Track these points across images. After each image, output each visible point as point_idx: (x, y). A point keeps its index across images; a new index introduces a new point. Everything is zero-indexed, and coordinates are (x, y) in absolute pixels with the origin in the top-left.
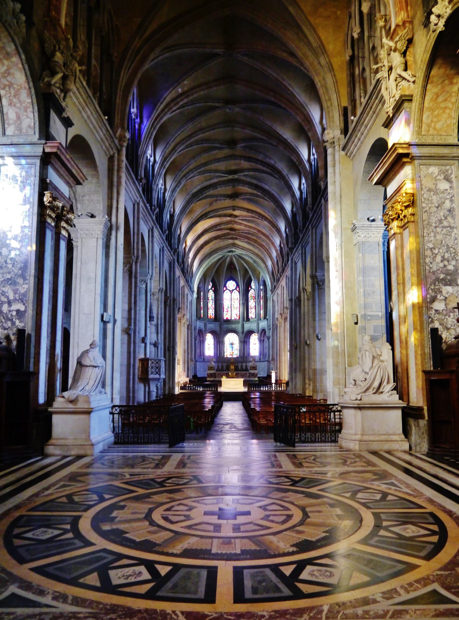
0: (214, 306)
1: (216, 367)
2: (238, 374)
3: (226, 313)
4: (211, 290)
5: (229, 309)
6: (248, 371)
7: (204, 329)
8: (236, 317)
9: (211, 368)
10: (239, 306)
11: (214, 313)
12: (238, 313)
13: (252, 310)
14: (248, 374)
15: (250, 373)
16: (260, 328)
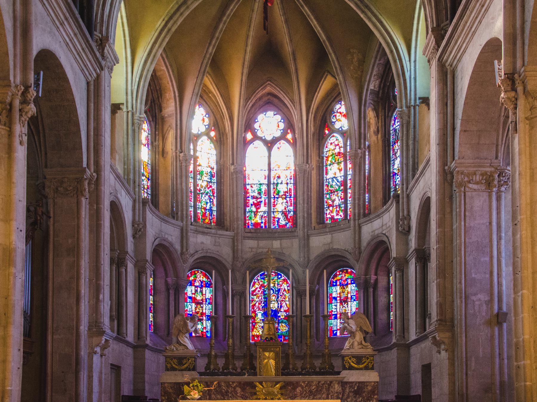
0: (214, 187)
1: (202, 363)
2: (295, 385)
3: (254, 209)
4: (205, 138)
5: (263, 198)
6: (338, 373)
7: (178, 247)
8: (283, 222)
9: (181, 360)
10: (291, 186)
11: (214, 208)
12: (292, 208)
13: (334, 197)
14: (337, 387)
15: (343, 384)
16: (364, 243)
